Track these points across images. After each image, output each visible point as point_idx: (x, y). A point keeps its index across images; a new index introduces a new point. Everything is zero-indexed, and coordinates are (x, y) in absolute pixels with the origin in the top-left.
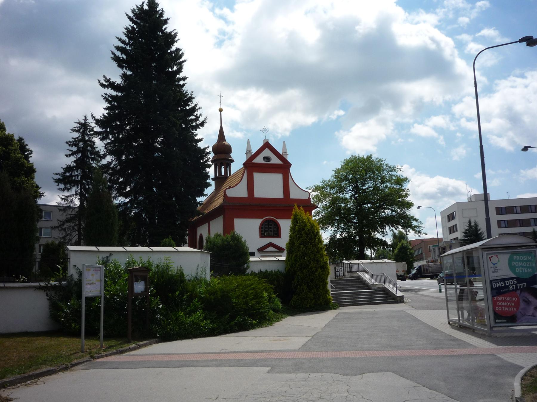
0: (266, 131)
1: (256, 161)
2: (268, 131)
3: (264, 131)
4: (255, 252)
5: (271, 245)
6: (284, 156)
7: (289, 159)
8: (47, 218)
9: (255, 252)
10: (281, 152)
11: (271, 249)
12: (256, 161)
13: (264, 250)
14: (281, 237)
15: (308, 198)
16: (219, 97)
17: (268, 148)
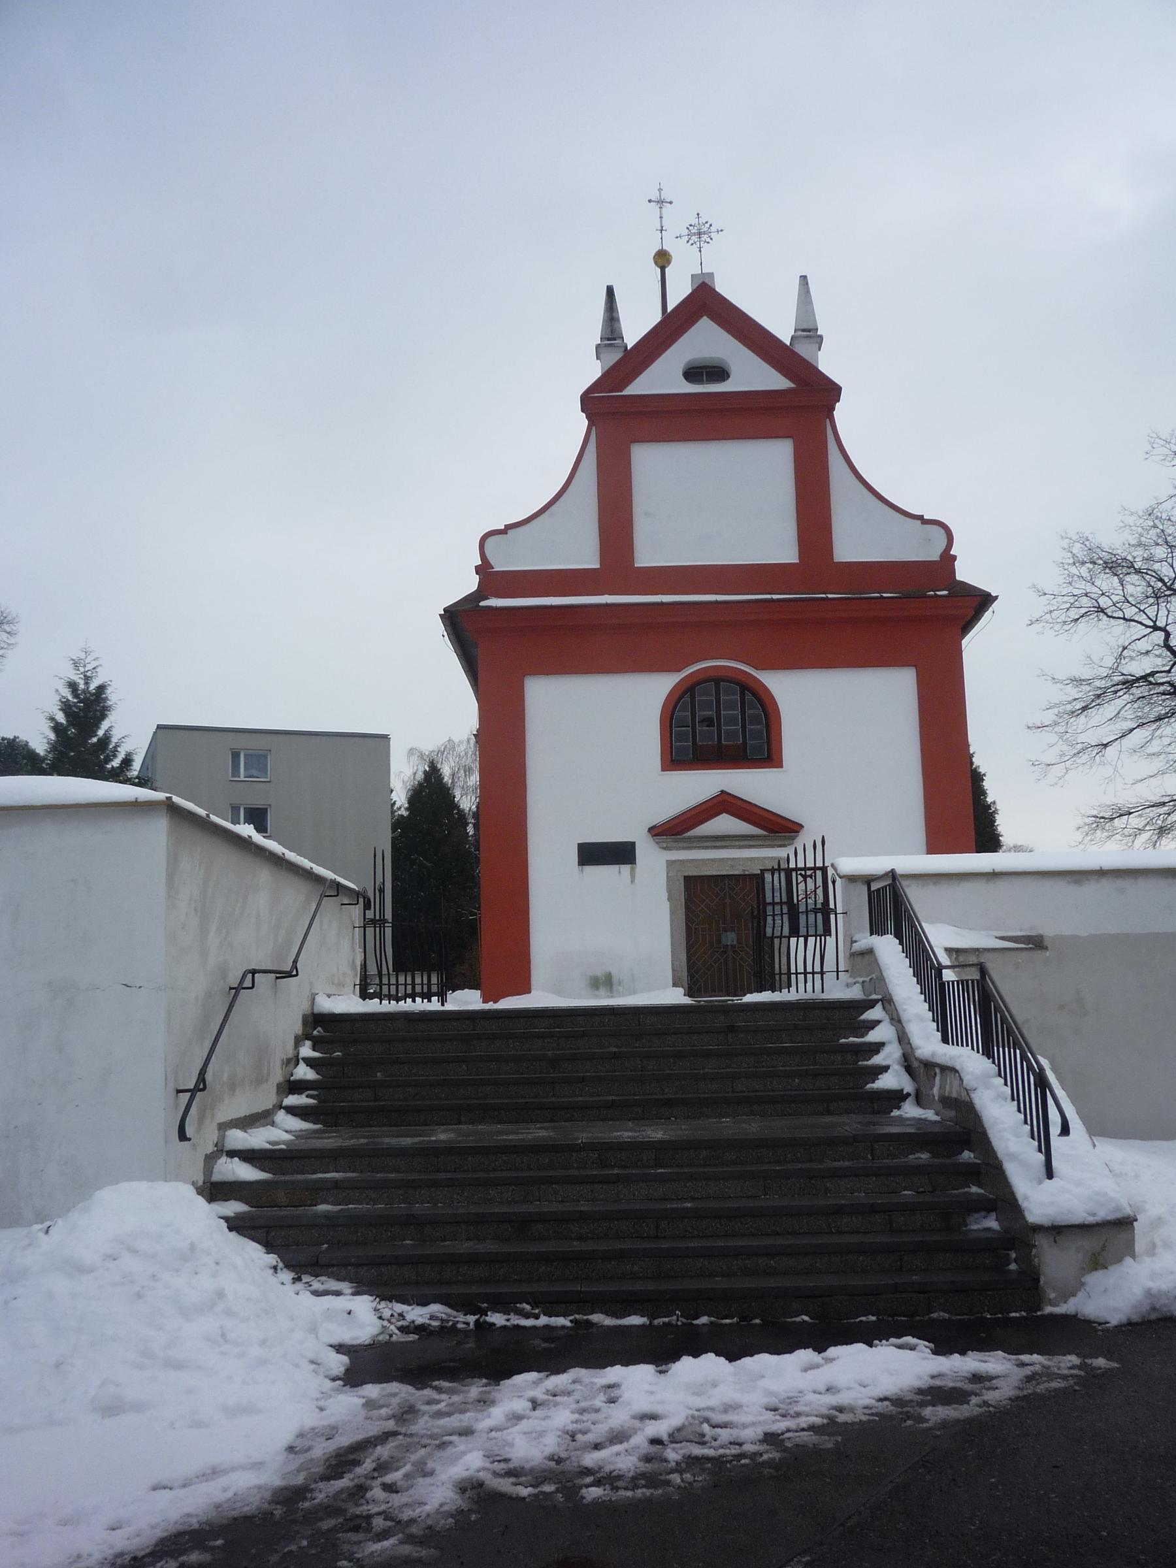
0: (705, 237)
1: (642, 386)
2: (713, 235)
3: (695, 238)
4: (633, 844)
5: (725, 803)
6: (803, 350)
7: (828, 363)
8: (255, 775)
9: (633, 844)
10: (784, 331)
11: (725, 824)
12: (642, 386)
13: (688, 831)
14: (782, 767)
15: (941, 556)
16: (654, 207)
17: (712, 319)
